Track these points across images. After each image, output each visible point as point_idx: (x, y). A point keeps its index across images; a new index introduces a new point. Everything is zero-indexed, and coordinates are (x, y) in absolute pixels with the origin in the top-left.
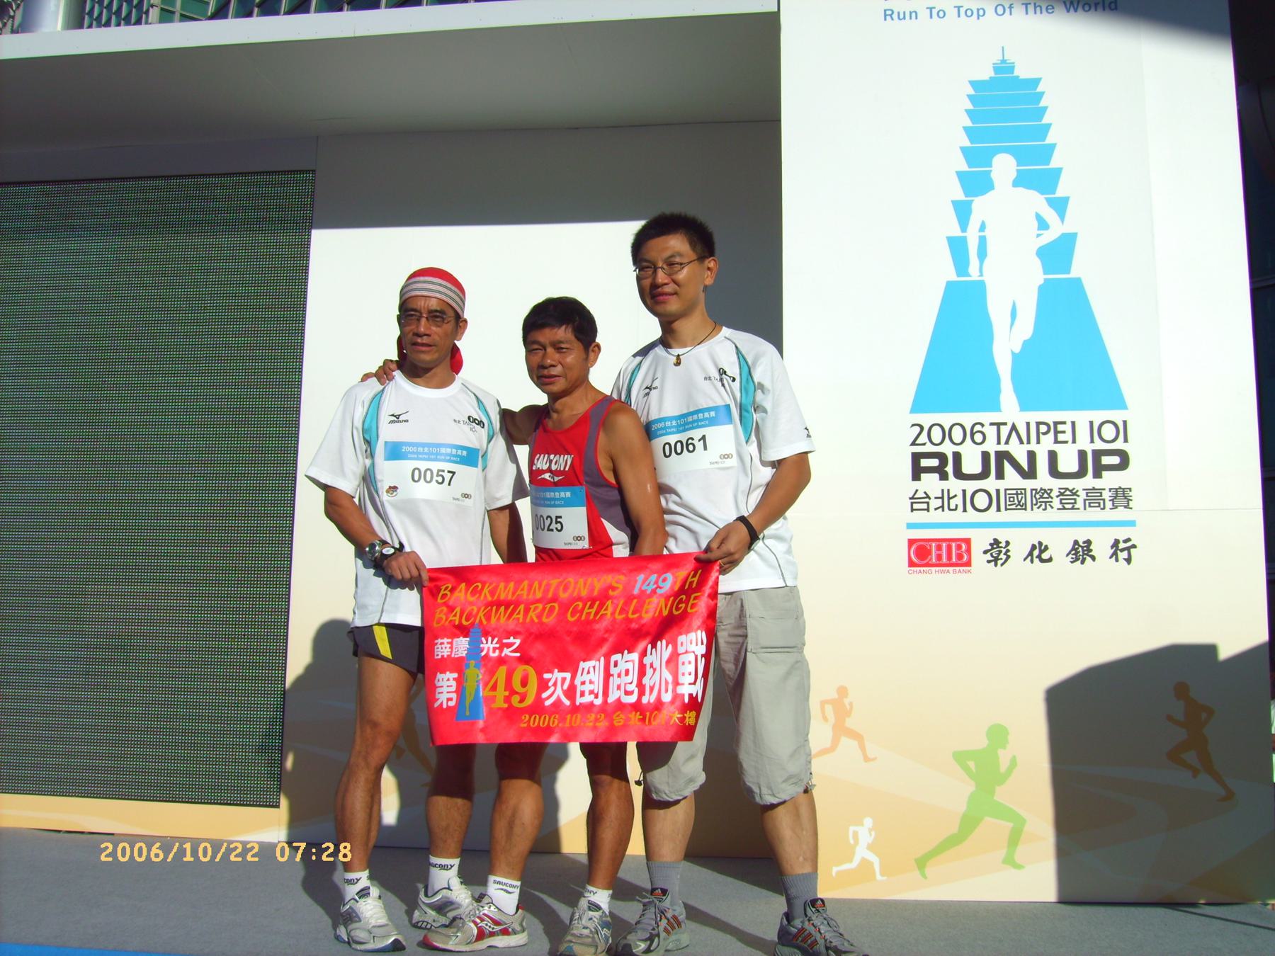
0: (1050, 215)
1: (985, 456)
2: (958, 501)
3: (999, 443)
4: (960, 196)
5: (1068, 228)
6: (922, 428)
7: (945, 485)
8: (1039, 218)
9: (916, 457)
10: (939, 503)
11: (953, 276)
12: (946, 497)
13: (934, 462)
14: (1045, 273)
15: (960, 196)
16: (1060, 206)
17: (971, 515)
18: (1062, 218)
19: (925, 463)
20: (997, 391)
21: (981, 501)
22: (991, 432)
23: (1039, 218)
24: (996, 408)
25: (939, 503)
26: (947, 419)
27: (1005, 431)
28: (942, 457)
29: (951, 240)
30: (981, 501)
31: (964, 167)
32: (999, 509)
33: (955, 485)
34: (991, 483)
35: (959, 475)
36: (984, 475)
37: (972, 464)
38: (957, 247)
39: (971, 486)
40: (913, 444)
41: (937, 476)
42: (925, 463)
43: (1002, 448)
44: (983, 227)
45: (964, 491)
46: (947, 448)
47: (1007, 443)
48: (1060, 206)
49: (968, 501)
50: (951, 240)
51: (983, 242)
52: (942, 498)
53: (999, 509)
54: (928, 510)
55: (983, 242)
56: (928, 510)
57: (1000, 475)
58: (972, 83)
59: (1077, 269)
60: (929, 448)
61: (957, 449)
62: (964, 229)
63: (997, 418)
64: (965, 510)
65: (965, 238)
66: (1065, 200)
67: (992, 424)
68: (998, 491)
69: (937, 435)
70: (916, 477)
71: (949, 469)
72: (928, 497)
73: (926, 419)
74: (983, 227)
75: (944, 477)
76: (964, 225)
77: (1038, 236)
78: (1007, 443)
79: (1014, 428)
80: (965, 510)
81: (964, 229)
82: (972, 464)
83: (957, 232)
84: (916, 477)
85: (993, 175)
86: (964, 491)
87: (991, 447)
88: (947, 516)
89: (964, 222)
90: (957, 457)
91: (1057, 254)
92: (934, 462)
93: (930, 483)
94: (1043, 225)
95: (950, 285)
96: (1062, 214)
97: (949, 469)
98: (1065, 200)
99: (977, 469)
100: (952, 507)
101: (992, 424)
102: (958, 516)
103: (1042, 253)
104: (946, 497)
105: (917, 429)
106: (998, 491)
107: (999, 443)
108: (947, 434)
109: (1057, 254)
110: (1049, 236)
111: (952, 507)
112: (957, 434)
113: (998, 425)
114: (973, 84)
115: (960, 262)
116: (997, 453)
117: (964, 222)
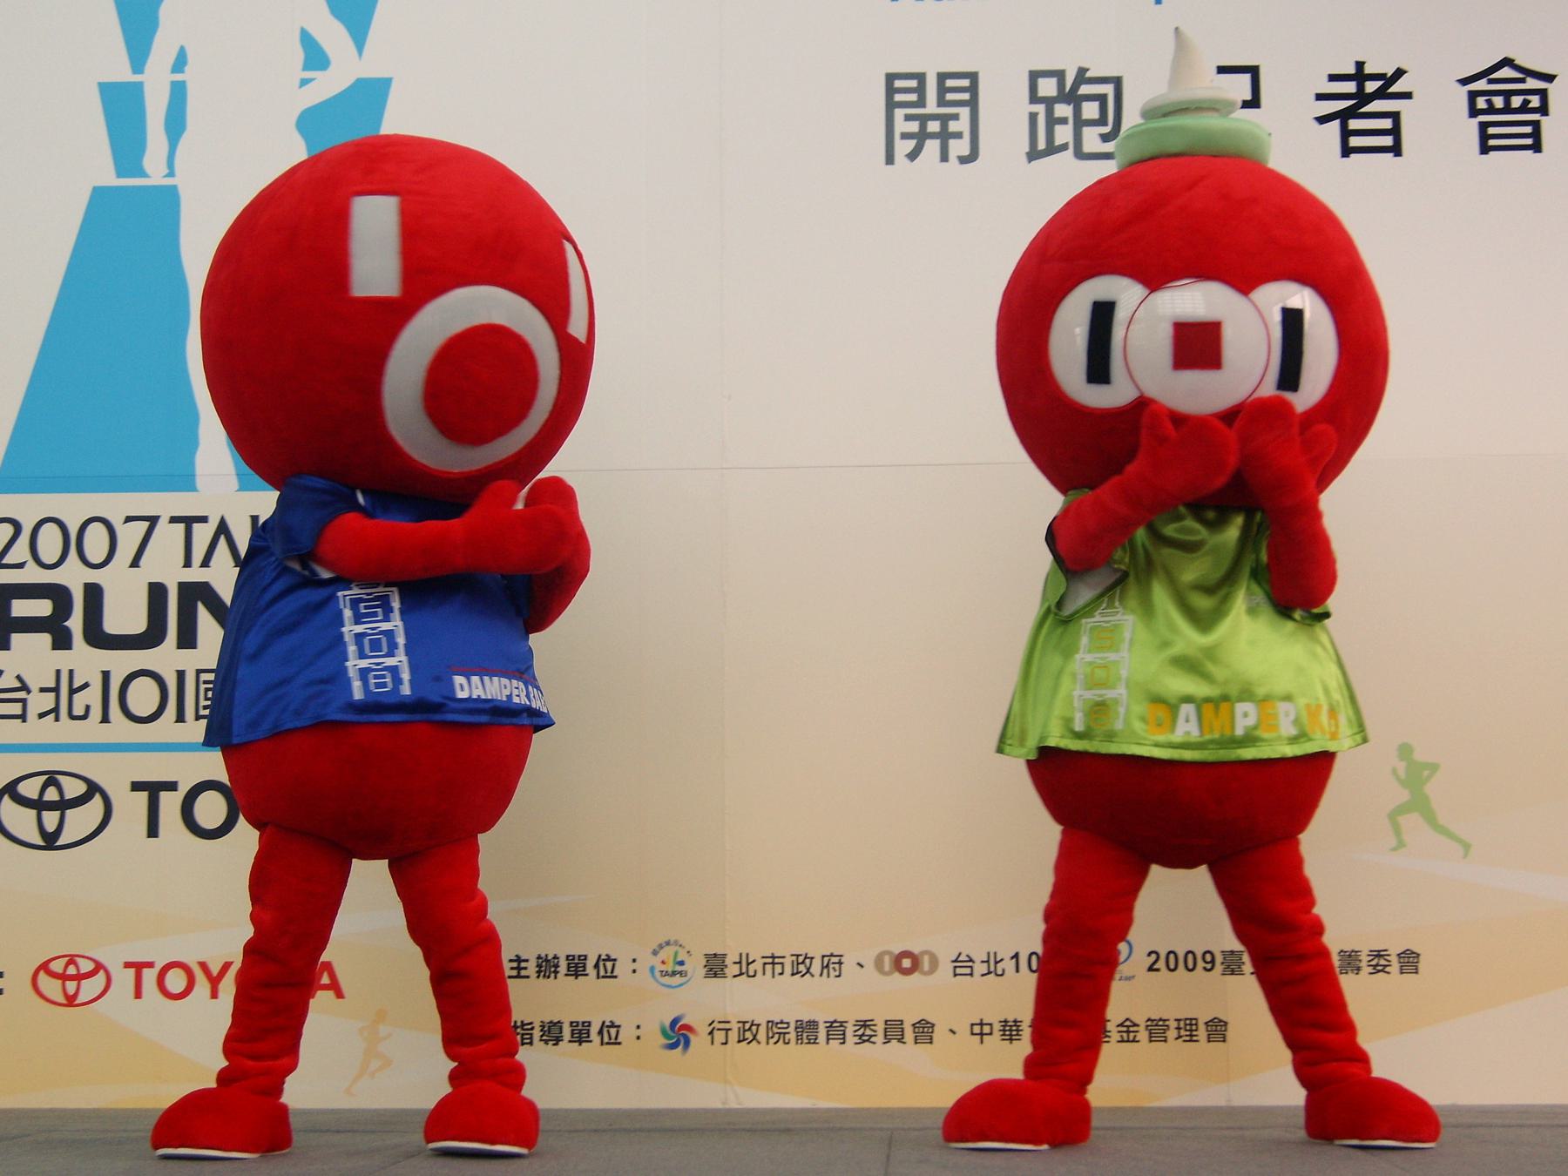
0: (334, 36)
1: (157, 593)
2: (92, 697)
3: (188, 563)
5: (371, 66)
6: (17, 527)
7: (63, 659)
8: (307, 40)
10: (48, 701)
11: (110, 179)
12: (64, 688)
13: (43, 608)
18: (359, 35)
20: (193, 442)
21: (143, 697)
22: (169, 538)
23: (307, 40)
24: (185, 481)
25: (48, 701)
26: (73, 507)
27: (203, 534)
28: (58, 595)
29: (110, 93)
30: (143, 697)
32: (180, 718)
33: (85, 660)
34: (166, 657)
35: (98, 637)
36: (151, 638)
37: (125, 615)
38: (122, 107)
39: (122, 662)
41: (45, 639)
43: (195, 575)
44: (180, 63)
45: (106, 675)
46: (73, 577)
47: (206, 563)
49: (114, 695)
50: (110, 93)
51: (178, 93)
52: (56, 690)
53: (180, 718)
54: (23, 717)
55: (178, 93)
56: (23, 717)
57: (187, 639)
60: (32, 575)
62: (138, 64)
63: (185, 504)
64: (105, 719)
65: (141, 84)
67: (174, 520)
68: (181, 675)
71: (75, 623)
72: (24, 687)
74: (180, 63)
75: (62, 641)
76: (138, 54)
77: (304, 82)
78: (206, 563)
79: (223, 529)
80: (105, 719)
81: (138, 64)
82: (125, 615)
83: (122, 72)
86: (106, 675)
87: (173, 575)
88: (67, 731)
90: (94, 594)
92: (43, 608)
94: (315, 58)
95: (99, 194)
96: (359, 35)
97: (75, 623)
99: (136, 623)
100: (79, 710)
101: (174, 520)
102: (91, 731)
104: (64, 688)
105: (8, 530)
106: (181, 675)
107: (188, 563)
108: (73, 543)
110: (329, 85)
111: (79, 710)
113: (189, 522)
116: (184, 588)
117: (138, 54)
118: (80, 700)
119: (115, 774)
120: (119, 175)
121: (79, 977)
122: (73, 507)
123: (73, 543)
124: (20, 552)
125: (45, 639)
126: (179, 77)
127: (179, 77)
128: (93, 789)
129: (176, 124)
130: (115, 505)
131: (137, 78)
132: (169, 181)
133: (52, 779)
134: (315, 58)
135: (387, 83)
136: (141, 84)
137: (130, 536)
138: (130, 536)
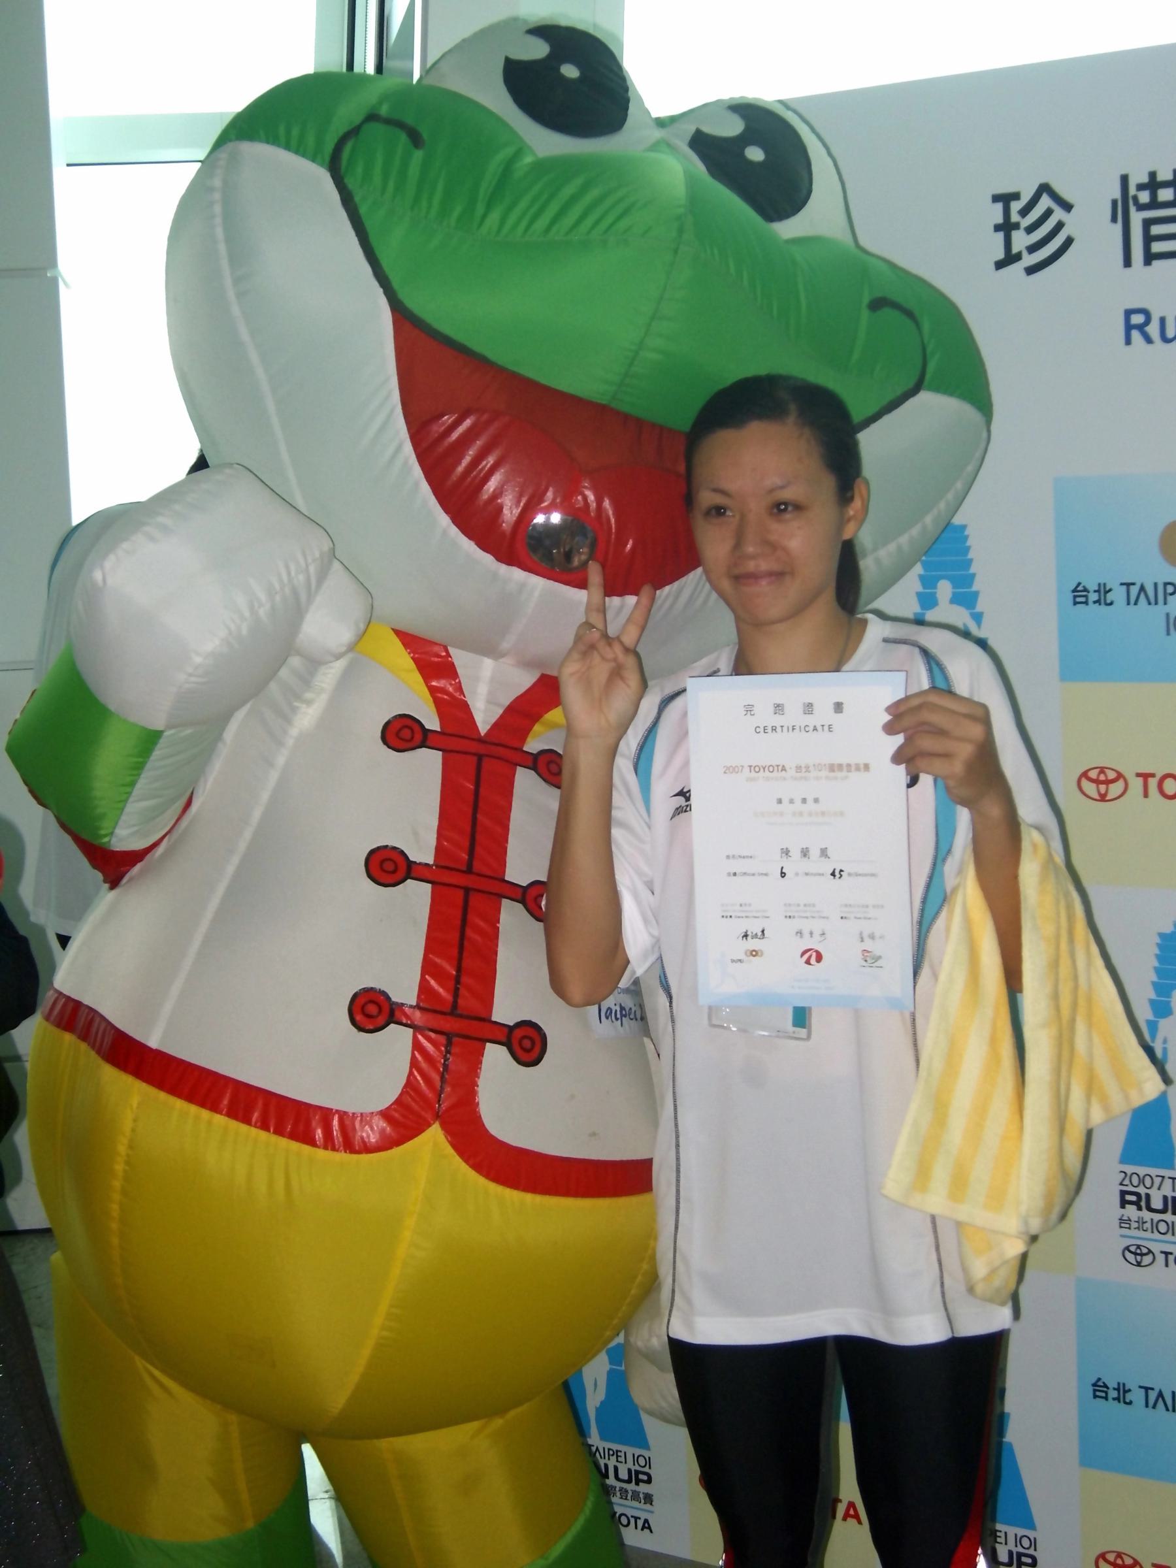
1: (1165, 1198)
2: (1148, 1225)
4: (1151, 1017)
9: (1123, 1193)
10: (1136, 1225)
12: (1141, 1222)
13: (1133, 1198)
15: (1151, 1017)
17: (1156, 1236)
19: (1128, 1198)
21: (1163, 1227)
25: (1136, 1225)
26: (1142, 1171)
28: (1138, 1195)
30: (1163, 1227)
31: (1153, 996)
33: (1147, 1215)
37: (1157, 1203)
39: (1157, 1217)
40: (1121, 1184)
42: (1128, 1198)
44: (1165, 1041)
46: (1142, 1190)
49: (1155, 1227)
58: (1161, 935)
61: (1148, 1191)
69: (1135, 1180)
70: (1123, 1207)
71: (1143, 1204)
73: (1130, 1169)
74: (1165, 1041)
75: (1140, 1209)
82: (1157, 1203)
84: (1123, 1207)
85: (1173, 1005)
88: (1142, 1234)
90: (1148, 1196)
92: (1133, 1198)
93: (1131, 1211)
97: (1143, 1204)
102: (1148, 1235)
108: (1142, 1181)
112: (1148, 1182)
114: (1161, 935)
118: (1146, 1226)
119: (1156, 1248)
121: (1142, 1255)
122: (1142, 1171)
123: (1142, 1181)
124: (1127, 1182)
125: (1134, 1207)
128: (1150, 1251)
130: (1154, 1172)
133: (1138, 1247)
137: (1157, 1181)
138: (1157, 1181)
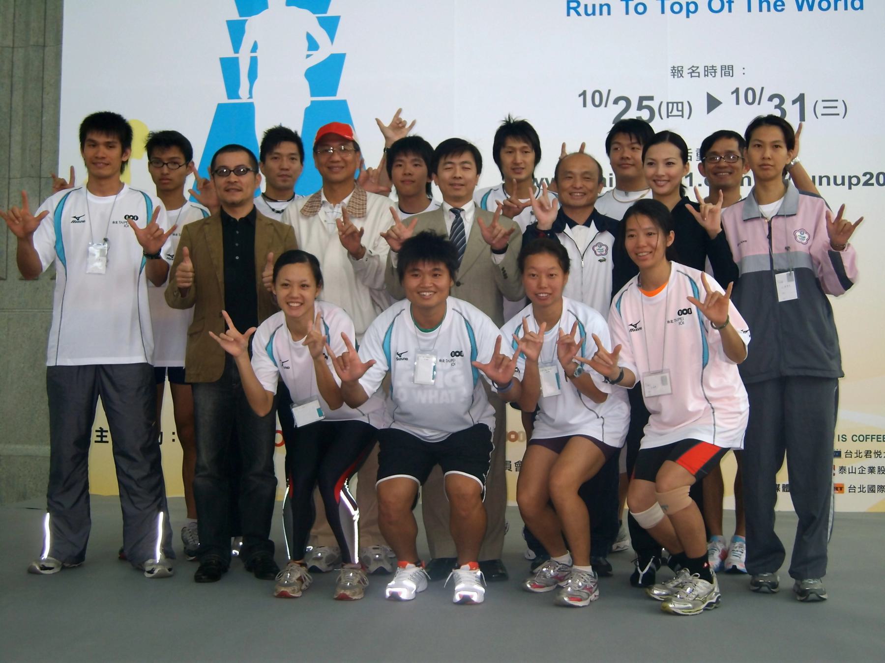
0: (320, 35)
5: (336, 49)
8: (309, 37)
14: (312, 95)
16: (330, 25)
23: (309, 37)
38: (229, 67)
44: (255, 48)
48: (330, 25)
51: (254, 61)
55: (254, 61)
59: (347, 89)
62: (236, 49)
65: (237, 58)
66: (336, 19)
74: (255, 48)
77: (308, 56)
81: (236, 49)
83: (229, 53)
89: (237, 43)
91: (325, 75)
94: (313, 45)
98: (336, 19)
103: (312, 74)
109: (325, 75)
110: (319, 57)
115: (232, 87)
117: (237, 43)
120: (229, 97)
126: (254, 54)
127: (254, 54)
129: (253, 75)
131: (236, 55)
132: (250, 101)
134: (313, 45)
135: (344, 55)
136: (237, 58)
